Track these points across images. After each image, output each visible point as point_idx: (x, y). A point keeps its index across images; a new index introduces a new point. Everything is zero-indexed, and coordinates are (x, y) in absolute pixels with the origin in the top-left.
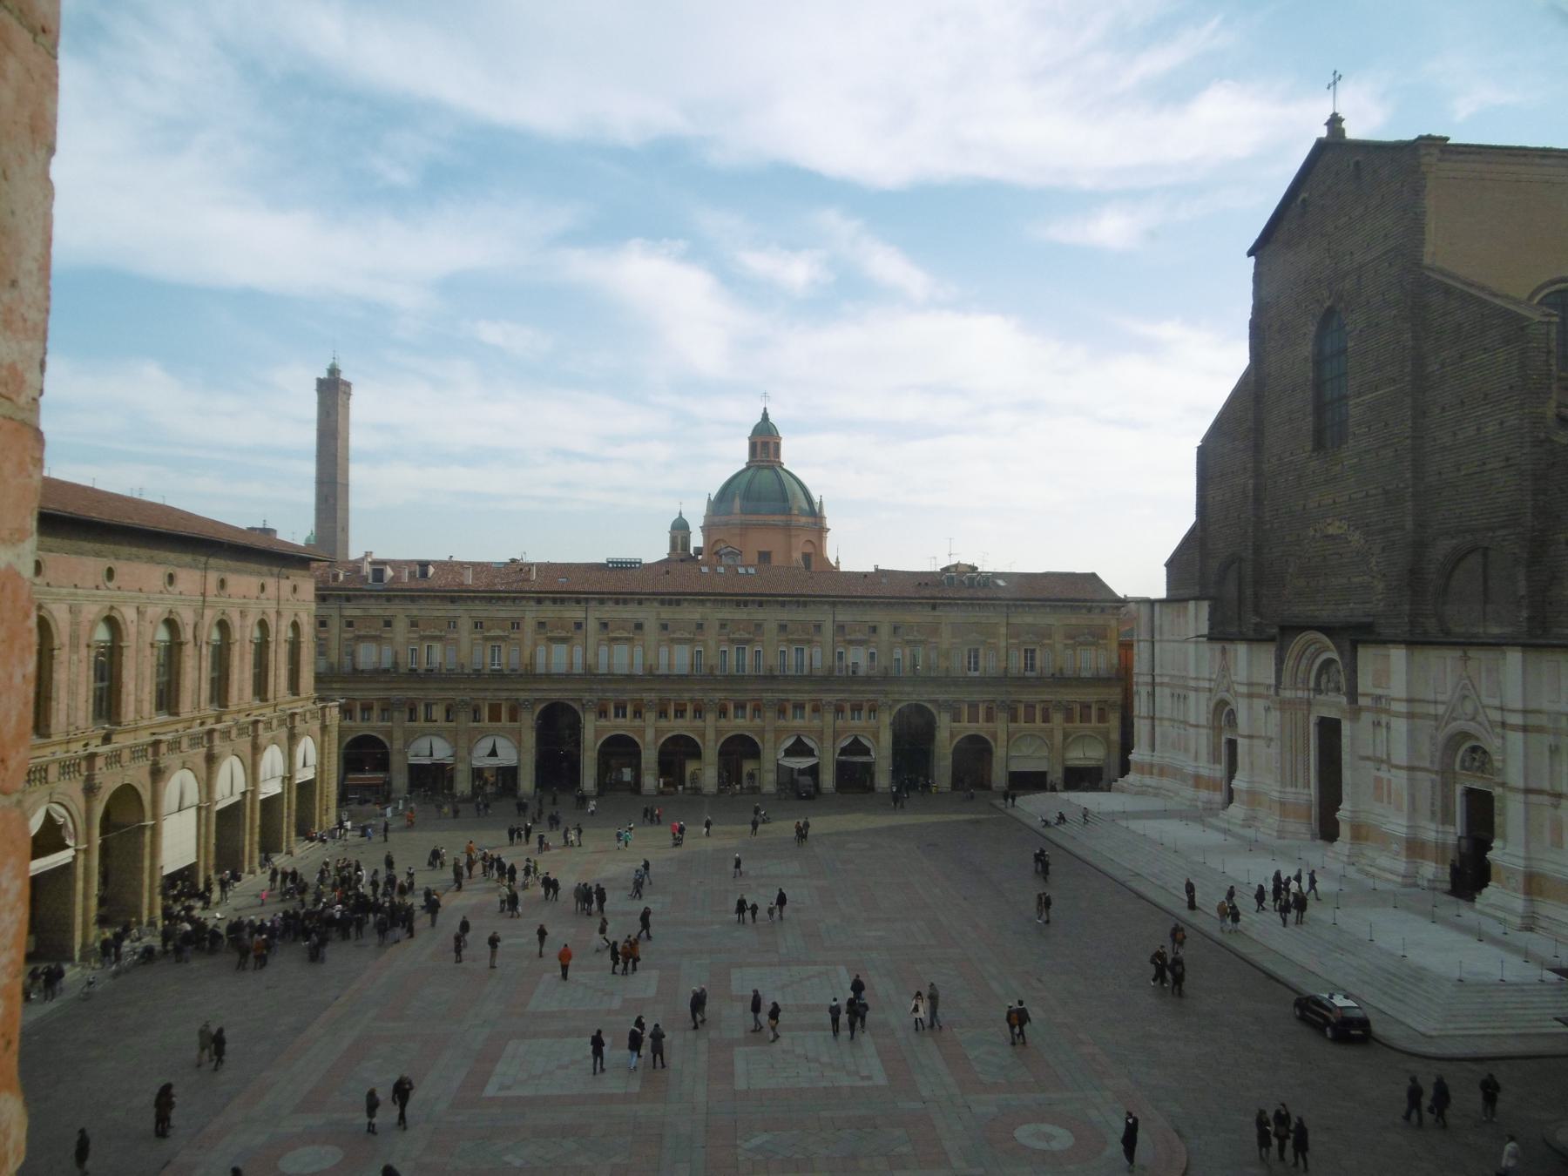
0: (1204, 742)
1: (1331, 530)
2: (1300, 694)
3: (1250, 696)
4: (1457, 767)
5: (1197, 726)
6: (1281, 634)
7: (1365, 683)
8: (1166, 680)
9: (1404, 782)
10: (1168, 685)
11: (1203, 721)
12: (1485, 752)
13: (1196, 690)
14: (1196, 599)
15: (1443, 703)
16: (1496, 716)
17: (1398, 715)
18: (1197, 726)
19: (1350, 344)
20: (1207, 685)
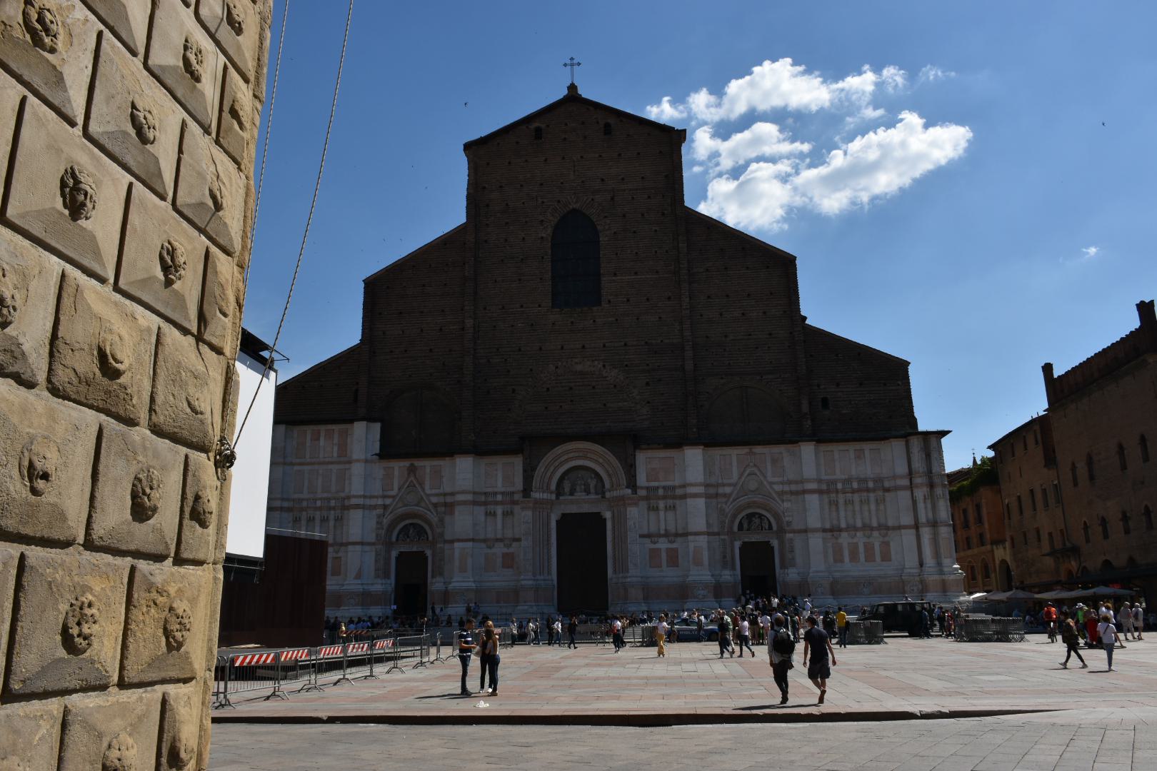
0: (370, 559)
1: (579, 368)
2: (545, 496)
3: (474, 503)
4: (735, 528)
5: (362, 544)
6: (529, 445)
7: (642, 479)
8: (286, 504)
9: (705, 545)
10: (289, 510)
11: (371, 538)
12: (761, 516)
13: (363, 507)
14: (370, 419)
15: (729, 485)
16: (787, 488)
17: (695, 496)
18: (362, 544)
19: (603, 239)
20: (380, 502)
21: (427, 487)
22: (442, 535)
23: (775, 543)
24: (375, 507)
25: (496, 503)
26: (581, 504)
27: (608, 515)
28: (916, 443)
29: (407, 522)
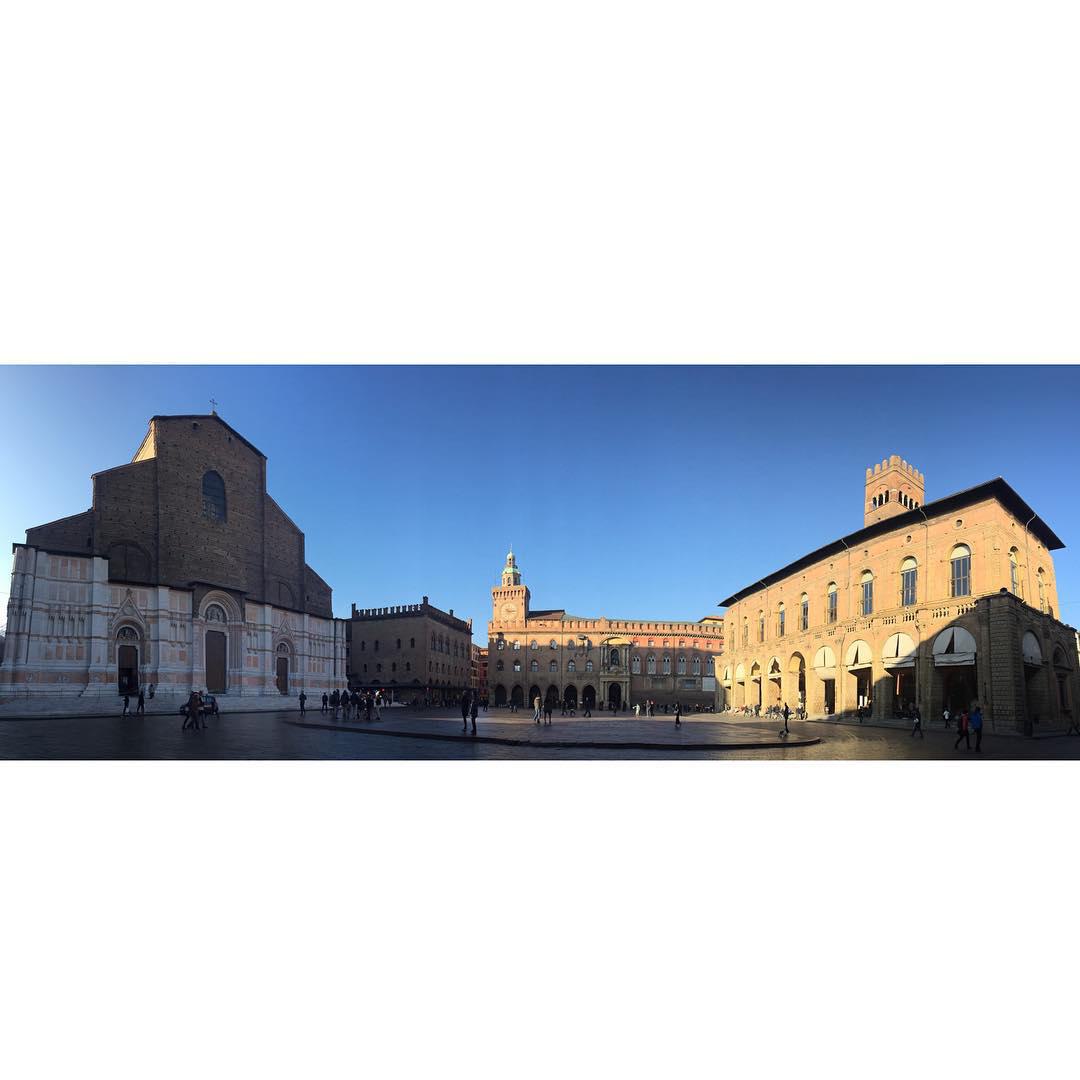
17: (268, 631)
20: (110, 611)
21: (138, 604)
22: (149, 636)
23: (289, 659)
24: (108, 614)
25: (177, 619)
26: (216, 625)
27: (228, 635)
28: (332, 623)
29: (124, 626)
